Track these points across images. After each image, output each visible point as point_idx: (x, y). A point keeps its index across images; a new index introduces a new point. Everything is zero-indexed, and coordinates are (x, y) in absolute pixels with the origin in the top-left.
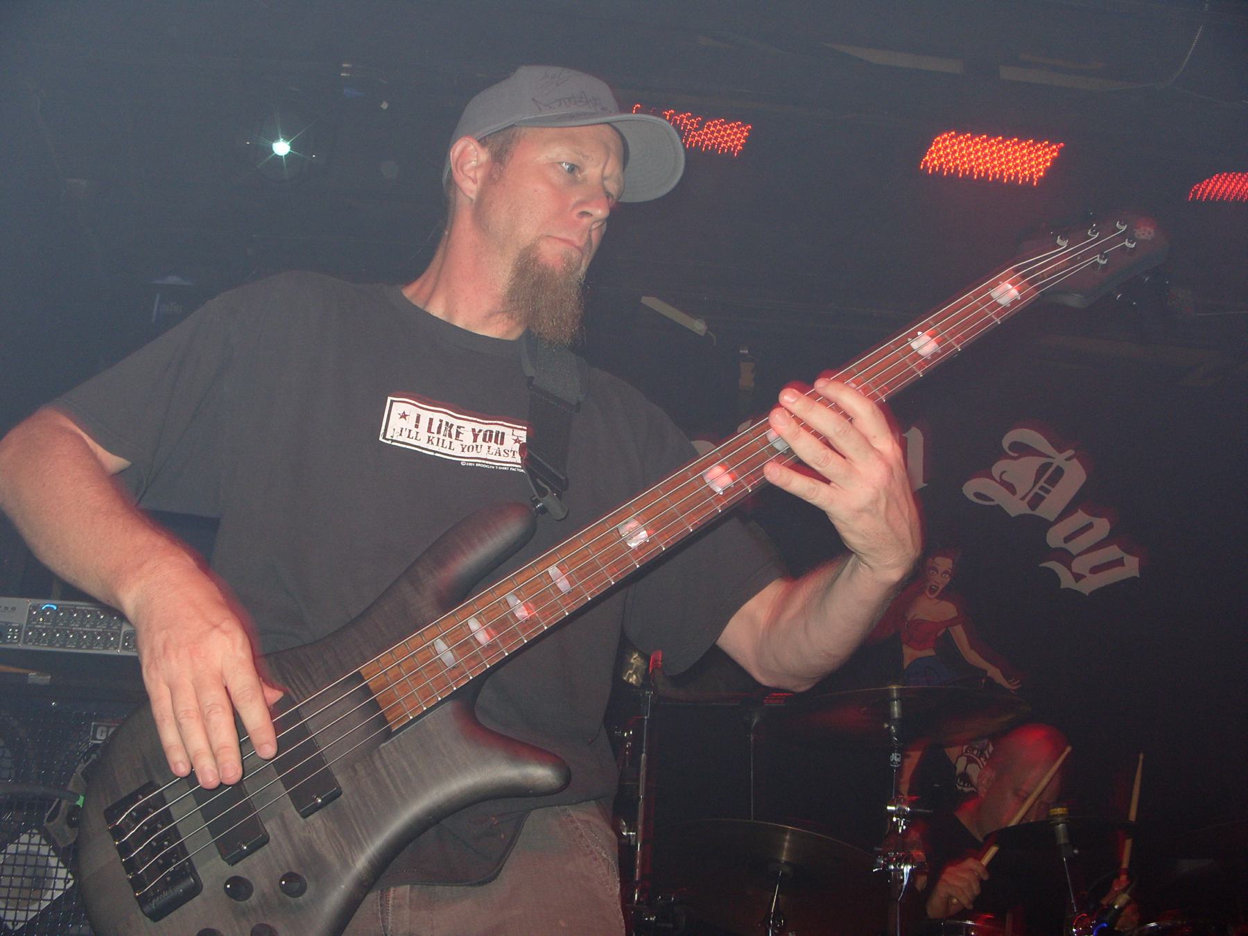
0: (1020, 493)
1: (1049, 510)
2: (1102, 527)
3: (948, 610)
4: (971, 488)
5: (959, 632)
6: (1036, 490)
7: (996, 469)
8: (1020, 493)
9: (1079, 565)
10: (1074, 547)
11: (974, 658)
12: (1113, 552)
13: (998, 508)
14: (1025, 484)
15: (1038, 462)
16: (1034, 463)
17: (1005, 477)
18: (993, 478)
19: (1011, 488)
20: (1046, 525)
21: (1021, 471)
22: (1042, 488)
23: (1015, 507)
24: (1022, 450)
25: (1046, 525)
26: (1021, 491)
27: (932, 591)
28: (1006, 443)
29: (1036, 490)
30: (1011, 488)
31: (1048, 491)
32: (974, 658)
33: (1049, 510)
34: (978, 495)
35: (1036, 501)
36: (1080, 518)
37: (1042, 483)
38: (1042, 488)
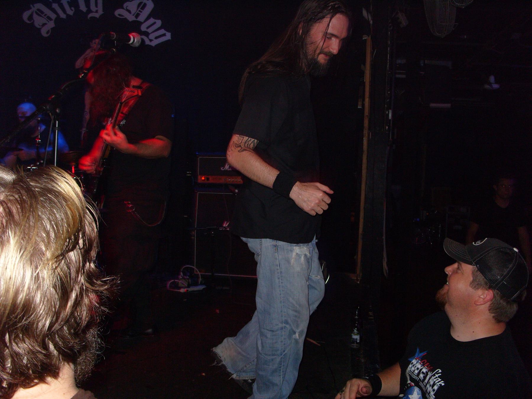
1: (141, 18)
2: (159, 23)
4: (118, 12)
7: (125, 5)
9: (152, 36)
10: (150, 30)
12: (162, 31)
13: (126, 19)
14: (134, 10)
18: (124, 9)
19: (129, 12)
20: (141, 23)
22: (139, 11)
25: (141, 23)
26: (133, 12)
30: (129, 12)
31: (141, 12)
33: (141, 18)
34: (119, 15)
35: (137, 16)
36: (152, 20)
37: (139, 9)
38: (139, 11)
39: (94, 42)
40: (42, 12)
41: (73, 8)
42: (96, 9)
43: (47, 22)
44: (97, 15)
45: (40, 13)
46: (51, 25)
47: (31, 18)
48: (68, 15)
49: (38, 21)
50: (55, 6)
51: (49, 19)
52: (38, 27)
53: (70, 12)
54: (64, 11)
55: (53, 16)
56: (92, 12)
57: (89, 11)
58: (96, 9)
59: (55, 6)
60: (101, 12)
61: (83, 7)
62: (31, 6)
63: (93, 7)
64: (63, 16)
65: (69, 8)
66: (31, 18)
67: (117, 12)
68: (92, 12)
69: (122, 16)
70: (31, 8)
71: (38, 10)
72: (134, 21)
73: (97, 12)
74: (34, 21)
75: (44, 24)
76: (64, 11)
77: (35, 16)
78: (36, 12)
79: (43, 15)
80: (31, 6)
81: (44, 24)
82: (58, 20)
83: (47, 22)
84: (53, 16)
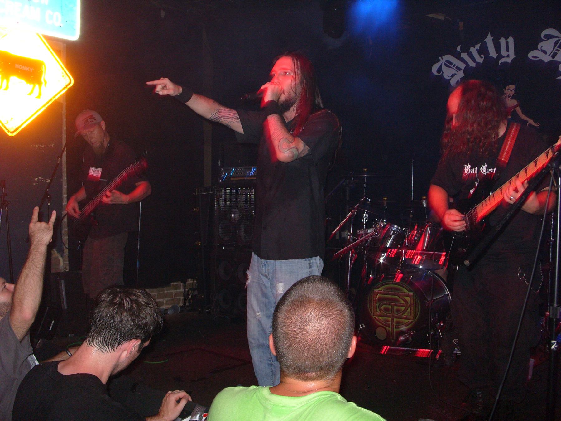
0: (548, 53)
3: (515, 102)
5: (518, 109)
6: (554, 51)
7: (539, 47)
8: (548, 53)
11: (524, 117)
13: (541, 61)
15: (554, 40)
16: (552, 41)
17: (543, 48)
19: (545, 52)
21: (548, 45)
22: (556, 50)
23: (546, 59)
24: (549, 37)
27: (509, 97)
28: (542, 36)
29: (554, 51)
30: (545, 52)
31: (559, 51)
32: (524, 117)
34: (533, 57)
37: (556, 48)
38: (556, 50)
39: (507, 88)
40: (451, 63)
41: (482, 56)
42: (508, 53)
43: (456, 72)
44: (509, 60)
45: (449, 64)
46: (461, 74)
47: (439, 70)
48: (478, 64)
49: (447, 73)
50: (464, 55)
51: (459, 69)
52: (448, 78)
53: (480, 60)
54: (473, 59)
55: (463, 66)
56: (504, 57)
57: (500, 56)
58: (508, 53)
59: (464, 55)
60: (512, 56)
61: (493, 53)
62: (440, 58)
63: (504, 52)
64: (472, 64)
65: (479, 56)
66: (439, 70)
67: (530, 55)
68: (504, 57)
69: (537, 58)
70: (439, 60)
71: (447, 61)
72: (550, 63)
73: (508, 56)
74: (443, 73)
75: (453, 75)
76: (473, 59)
77: (444, 68)
78: (445, 64)
79: (452, 66)
80: (440, 58)
81: (453, 75)
82: (468, 70)
83: (456, 72)
84: (463, 66)
